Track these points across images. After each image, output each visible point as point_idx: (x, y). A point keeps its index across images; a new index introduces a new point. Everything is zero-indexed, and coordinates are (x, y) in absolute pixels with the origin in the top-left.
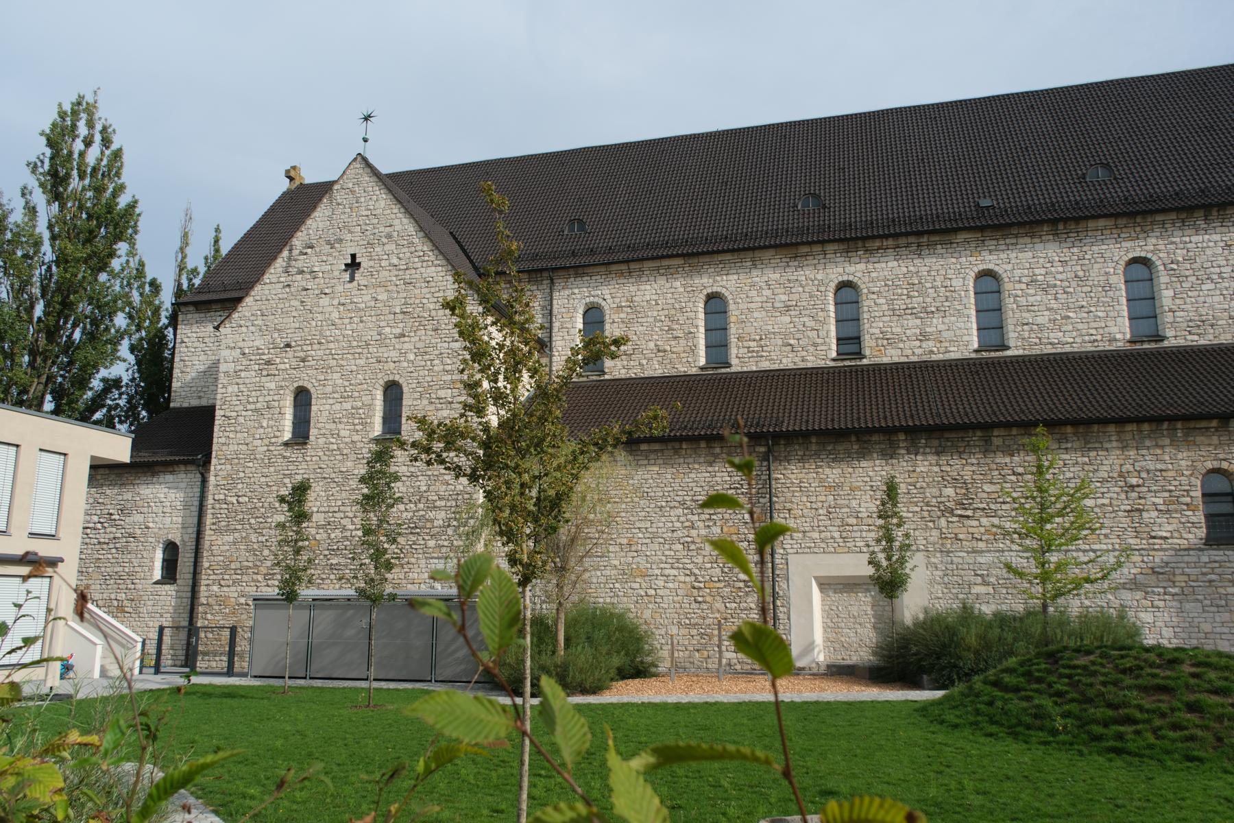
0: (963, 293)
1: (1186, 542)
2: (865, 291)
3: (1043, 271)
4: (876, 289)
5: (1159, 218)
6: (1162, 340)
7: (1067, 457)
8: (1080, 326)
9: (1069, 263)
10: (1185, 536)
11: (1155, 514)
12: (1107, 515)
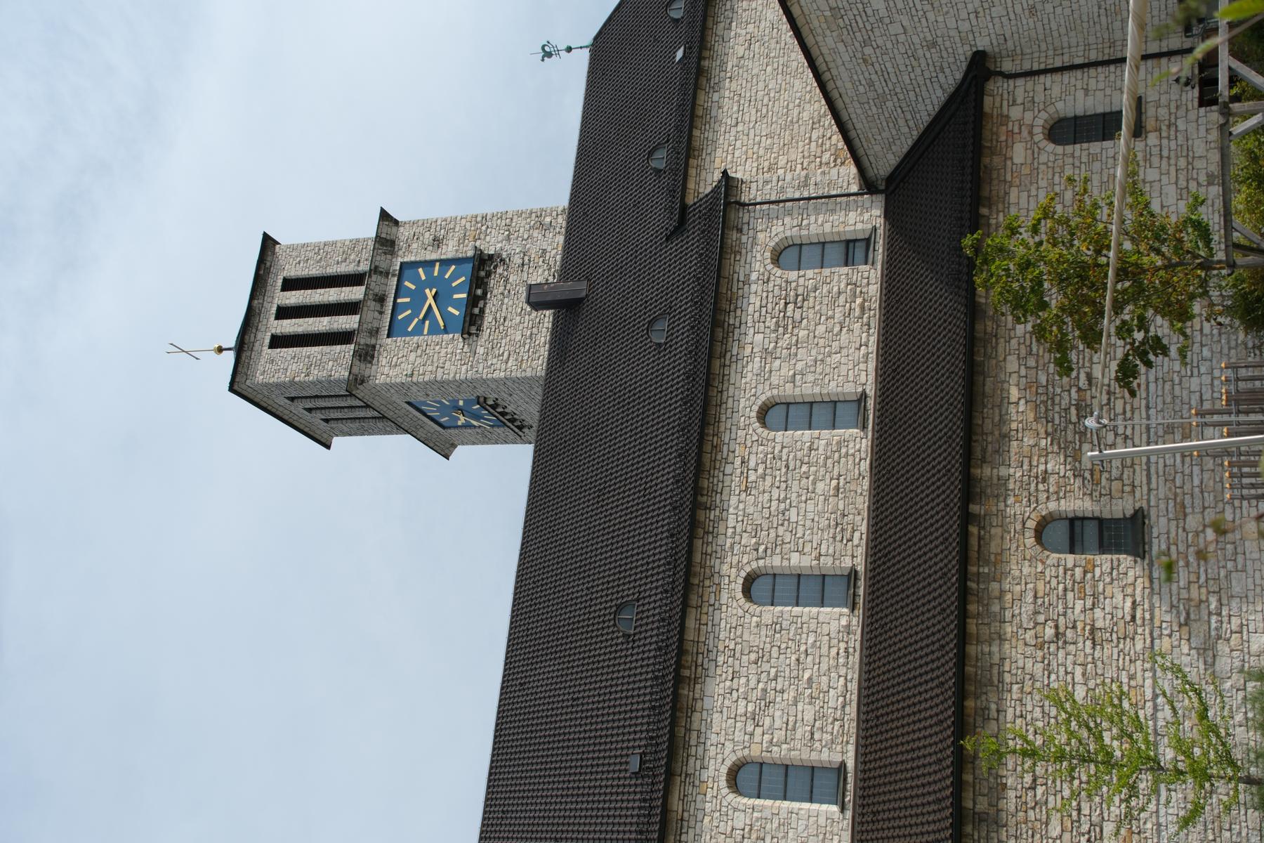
0: (755, 814)
1: (1140, 580)
3: (742, 703)
5: (697, 558)
6: (856, 572)
7: (1010, 712)
8: (824, 667)
9: (737, 669)
10: (1130, 580)
11: (1098, 613)
12: (1100, 672)
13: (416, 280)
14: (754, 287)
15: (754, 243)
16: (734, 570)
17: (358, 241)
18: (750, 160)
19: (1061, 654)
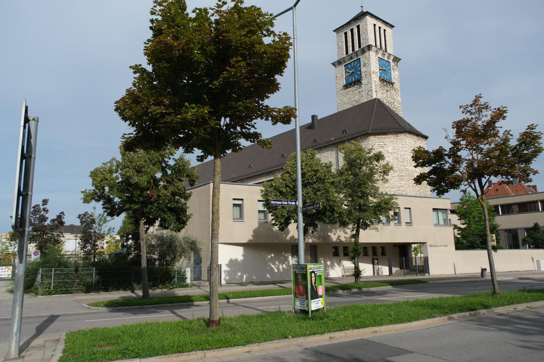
13: (357, 64)
17: (368, 40)
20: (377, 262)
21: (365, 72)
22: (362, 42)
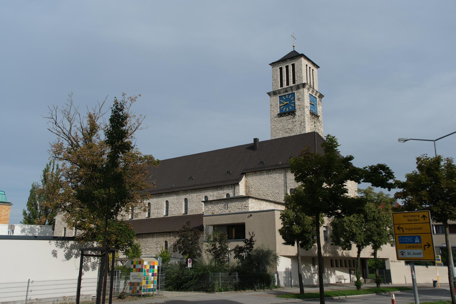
2: (151, 204)
3: (174, 201)
4: (152, 204)
5: (188, 191)
8: (177, 211)
11: (159, 248)
13: (291, 97)
14: (223, 191)
15: (229, 190)
16: (187, 196)
17: (302, 78)
18: (253, 183)
19: (155, 244)
20: (353, 272)
21: (299, 105)
22: (296, 79)
